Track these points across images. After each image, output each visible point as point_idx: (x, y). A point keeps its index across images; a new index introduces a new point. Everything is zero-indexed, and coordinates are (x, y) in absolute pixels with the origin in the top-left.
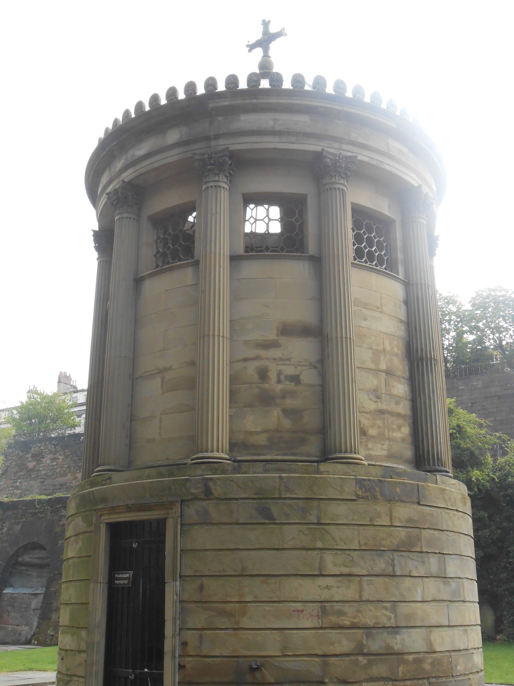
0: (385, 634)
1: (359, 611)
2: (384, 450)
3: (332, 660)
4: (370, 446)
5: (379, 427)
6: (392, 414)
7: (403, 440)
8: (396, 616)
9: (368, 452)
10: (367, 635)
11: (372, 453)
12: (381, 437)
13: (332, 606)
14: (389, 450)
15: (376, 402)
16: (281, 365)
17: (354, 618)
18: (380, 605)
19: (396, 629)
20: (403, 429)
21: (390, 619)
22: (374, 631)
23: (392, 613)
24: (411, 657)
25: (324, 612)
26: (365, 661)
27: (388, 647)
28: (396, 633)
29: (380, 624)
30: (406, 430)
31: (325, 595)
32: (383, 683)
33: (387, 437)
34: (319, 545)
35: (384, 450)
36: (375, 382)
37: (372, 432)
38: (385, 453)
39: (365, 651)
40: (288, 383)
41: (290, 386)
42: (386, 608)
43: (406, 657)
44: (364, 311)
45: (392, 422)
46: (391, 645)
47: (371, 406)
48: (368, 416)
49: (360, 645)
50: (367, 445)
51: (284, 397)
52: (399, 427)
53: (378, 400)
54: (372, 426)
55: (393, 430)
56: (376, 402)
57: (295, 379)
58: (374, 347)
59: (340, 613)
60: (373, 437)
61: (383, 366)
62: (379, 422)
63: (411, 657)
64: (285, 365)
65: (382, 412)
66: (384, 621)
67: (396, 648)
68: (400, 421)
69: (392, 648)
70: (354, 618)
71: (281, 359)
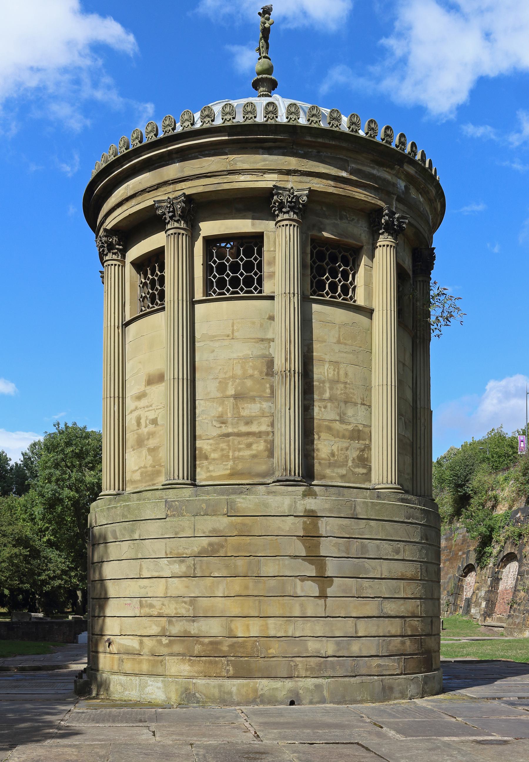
0: (184, 621)
1: (163, 605)
2: (227, 469)
3: (145, 639)
4: (211, 468)
5: (222, 450)
6: (239, 435)
7: (254, 456)
8: (194, 609)
9: (208, 474)
10: (170, 622)
11: (214, 474)
12: (225, 457)
13: (146, 601)
14: (232, 468)
15: (221, 427)
16: (147, 411)
17: (160, 609)
18: (180, 599)
19: (195, 618)
20: (254, 447)
21: (189, 610)
22: (174, 619)
23: (191, 606)
24: (207, 640)
25: (141, 606)
26: (167, 641)
27: (185, 631)
28: (194, 621)
29: (180, 614)
30: (260, 446)
31: (142, 593)
32: (181, 657)
33: (231, 457)
34: (140, 556)
35: (227, 469)
36: (220, 409)
37: (213, 455)
38: (228, 472)
39: (168, 634)
40: (151, 426)
41: (151, 427)
42: (185, 603)
43: (202, 639)
44: (211, 344)
45: (239, 442)
46: (188, 630)
47: (215, 432)
48: (211, 441)
49: (164, 629)
50: (208, 468)
51: (148, 439)
52: (249, 446)
53: (223, 425)
54: (214, 450)
55: (240, 450)
56: (221, 427)
57: (154, 422)
58: (222, 376)
59: (151, 606)
60: (214, 459)
61: (231, 391)
62: (223, 445)
63: (207, 640)
64: (149, 411)
65: (228, 435)
66: (183, 612)
67: (192, 632)
68: (251, 439)
69: (190, 632)
70: (160, 609)
71: (147, 407)
